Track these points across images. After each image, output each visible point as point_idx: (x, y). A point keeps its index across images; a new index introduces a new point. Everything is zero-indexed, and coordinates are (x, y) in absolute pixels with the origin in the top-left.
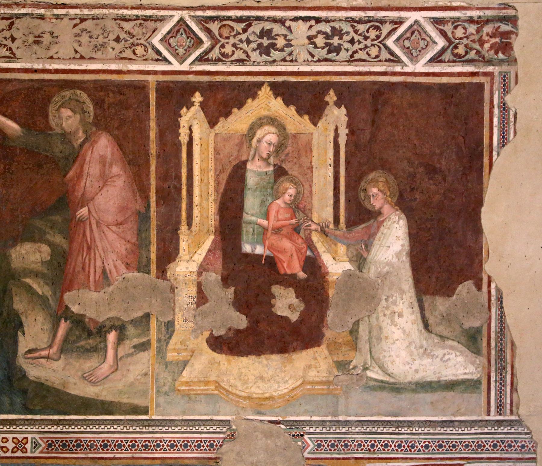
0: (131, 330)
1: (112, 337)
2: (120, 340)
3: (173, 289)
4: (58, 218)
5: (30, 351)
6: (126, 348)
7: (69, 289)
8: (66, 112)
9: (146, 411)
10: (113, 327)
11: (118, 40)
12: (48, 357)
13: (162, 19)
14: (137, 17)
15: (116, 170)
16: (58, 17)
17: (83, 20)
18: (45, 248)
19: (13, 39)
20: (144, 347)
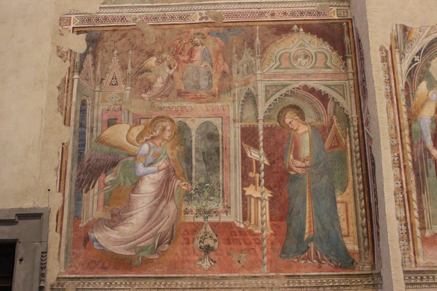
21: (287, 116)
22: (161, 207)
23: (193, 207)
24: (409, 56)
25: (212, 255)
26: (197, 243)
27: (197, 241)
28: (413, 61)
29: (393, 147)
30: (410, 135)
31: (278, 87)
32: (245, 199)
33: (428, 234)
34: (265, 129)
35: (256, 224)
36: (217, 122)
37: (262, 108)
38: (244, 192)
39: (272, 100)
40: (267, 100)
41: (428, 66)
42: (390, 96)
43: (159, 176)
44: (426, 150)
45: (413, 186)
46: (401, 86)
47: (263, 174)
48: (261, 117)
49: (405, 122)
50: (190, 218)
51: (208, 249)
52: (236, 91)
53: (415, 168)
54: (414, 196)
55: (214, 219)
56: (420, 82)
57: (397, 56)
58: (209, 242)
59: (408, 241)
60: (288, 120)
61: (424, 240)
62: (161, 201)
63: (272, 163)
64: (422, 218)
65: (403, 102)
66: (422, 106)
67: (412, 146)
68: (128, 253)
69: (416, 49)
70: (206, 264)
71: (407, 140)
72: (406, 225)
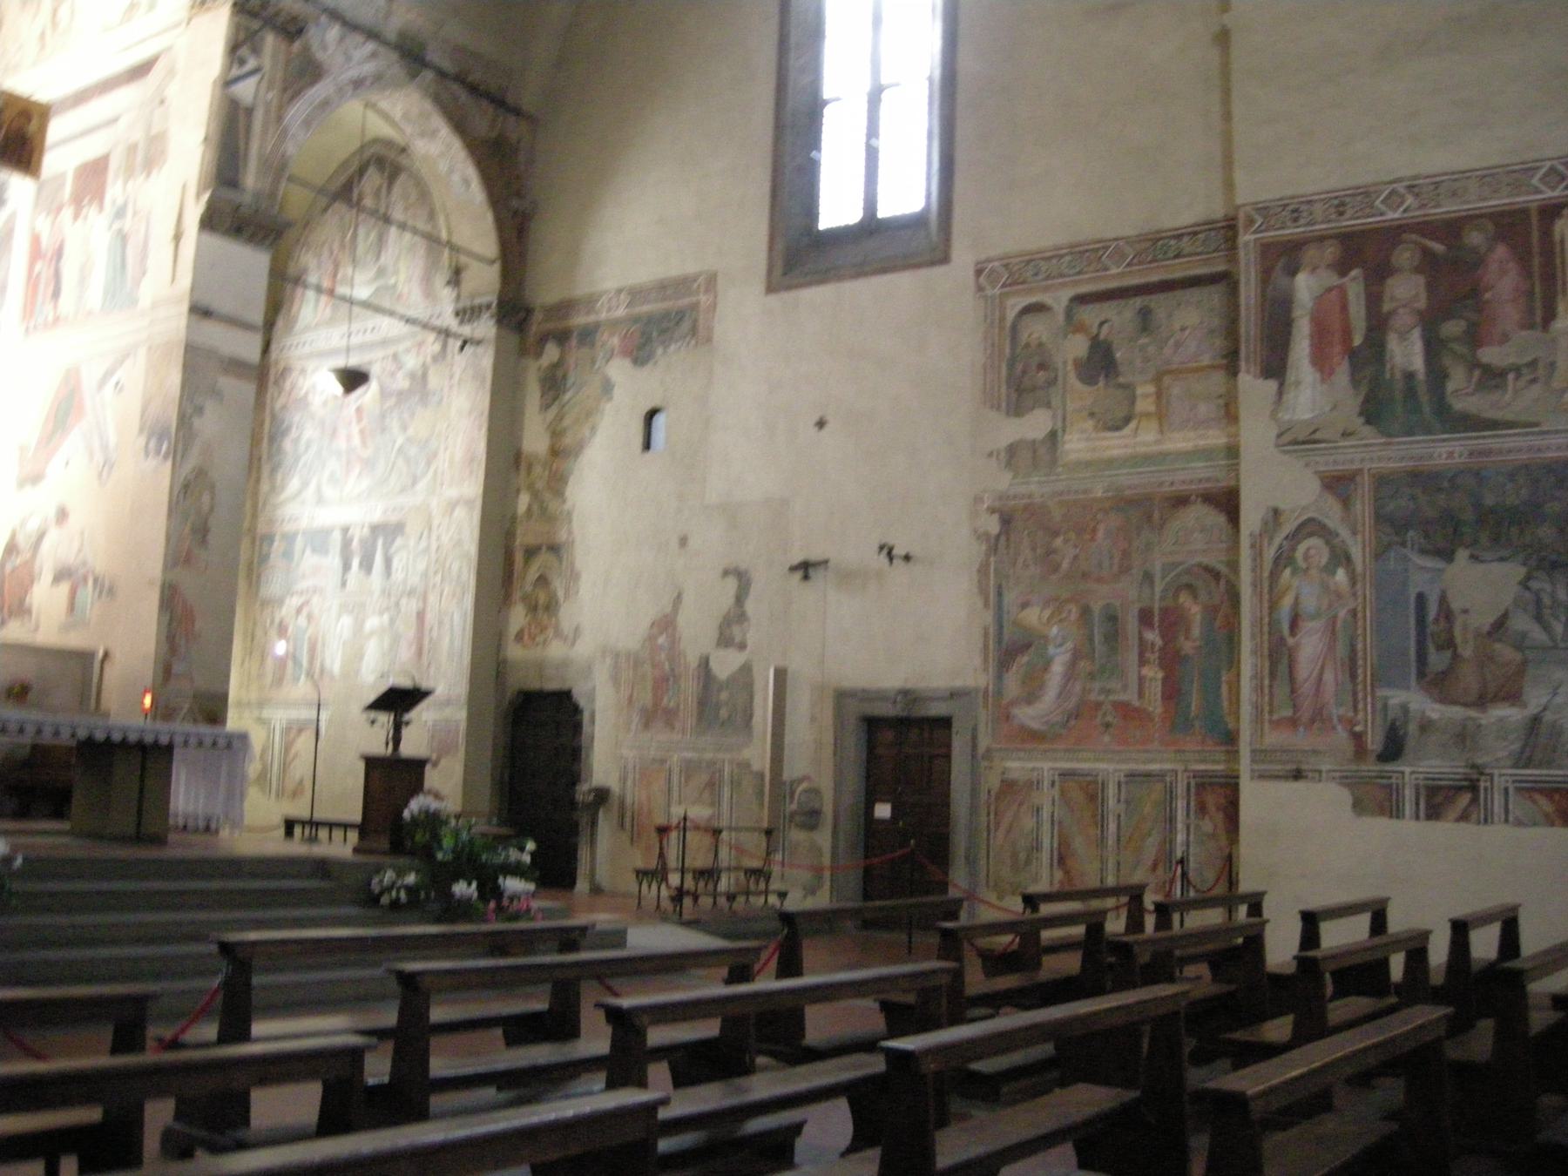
0: (1525, 371)
1: (1511, 376)
2: (1517, 378)
3: (1554, 340)
4: (1469, 302)
5: (1452, 393)
6: (1522, 383)
7: (1480, 346)
8: (1475, 234)
9: (1536, 425)
10: (1511, 370)
11: (1508, 185)
12: (1467, 394)
13: (1538, 168)
14: (1522, 169)
15: (1511, 265)
16: (1468, 178)
17: (1484, 176)
18: (1463, 323)
19: (1438, 195)
20: (1534, 381)
21: (1181, 595)
22: (1070, 685)
23: (1097, 685)
24: (1277, 540)
25: (1111, 729)
26: (1098, 720)
27: (1100, 717)
28: (1280, 547)
29: (1253, 636)
30: (1269, 624)
31: (1175, 565)
32: (1141, 679)
33: (1275, 717)
34: (1161, 609)
35: (1150, 701)
36: (1118, 603)
37: (1158, 588)
38: (1139, 672)
39: (1168, 579)
40: (1163, 578)
41: (1294, 549)
42: (1254, 585)
43: (1066, 657)
44: (1282, 639)
45: (1266, 672)
46: (1266, 574)
47: (1157, 655)
48: (1157, 597)
49: (1266, 612)
50: (1093, 697)
51: (1108, 725)
52: (1134, 571)
53: (1270, 656)
54: (1266, 682)
55: (1111, 698)
56: (1285, 567)
57: (1266, 542)
58: (1109, 718)
59: (1257, 722)
60: (1181, 600)
61: (1271, 722)
62: (1069, 680)
63: (1166, 644)
64: (1271, 704)
65: (1266, 590)
66: (1284, 593)
67: (1270, 633)
68: (1044, 728)
69: (1283, 535)
70: (1107, 739)
71: (1266, 629)
72: (1257, 708)
